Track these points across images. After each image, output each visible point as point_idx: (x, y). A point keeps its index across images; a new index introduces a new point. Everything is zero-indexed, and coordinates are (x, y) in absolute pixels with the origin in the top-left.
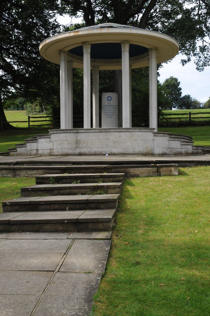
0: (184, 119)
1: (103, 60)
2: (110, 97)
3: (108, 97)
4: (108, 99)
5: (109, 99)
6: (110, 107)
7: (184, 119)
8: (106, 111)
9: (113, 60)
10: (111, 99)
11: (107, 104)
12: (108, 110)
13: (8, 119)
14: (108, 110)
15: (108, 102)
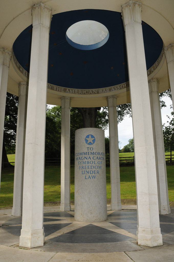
0: (130, 161)
1: (76, 90)
2: (92, 136)
3: (88, 137)
4: (87, 141)
5: (90, 140)
6: (92, 156)
7: (130, 161)
8: (84, 165)
9: (90, 90)
10: (94, 141)
11: (85, 150)
12: (88, 163)
13: (10, 161)
14: (88, 163)
15: (88, 146)
